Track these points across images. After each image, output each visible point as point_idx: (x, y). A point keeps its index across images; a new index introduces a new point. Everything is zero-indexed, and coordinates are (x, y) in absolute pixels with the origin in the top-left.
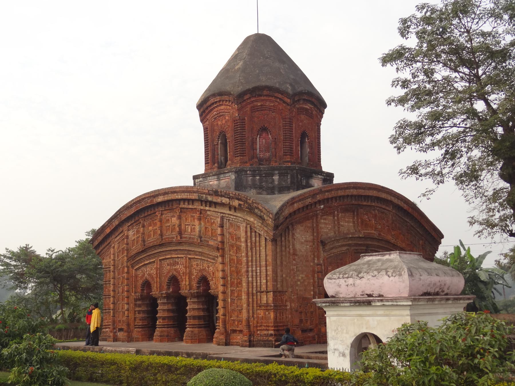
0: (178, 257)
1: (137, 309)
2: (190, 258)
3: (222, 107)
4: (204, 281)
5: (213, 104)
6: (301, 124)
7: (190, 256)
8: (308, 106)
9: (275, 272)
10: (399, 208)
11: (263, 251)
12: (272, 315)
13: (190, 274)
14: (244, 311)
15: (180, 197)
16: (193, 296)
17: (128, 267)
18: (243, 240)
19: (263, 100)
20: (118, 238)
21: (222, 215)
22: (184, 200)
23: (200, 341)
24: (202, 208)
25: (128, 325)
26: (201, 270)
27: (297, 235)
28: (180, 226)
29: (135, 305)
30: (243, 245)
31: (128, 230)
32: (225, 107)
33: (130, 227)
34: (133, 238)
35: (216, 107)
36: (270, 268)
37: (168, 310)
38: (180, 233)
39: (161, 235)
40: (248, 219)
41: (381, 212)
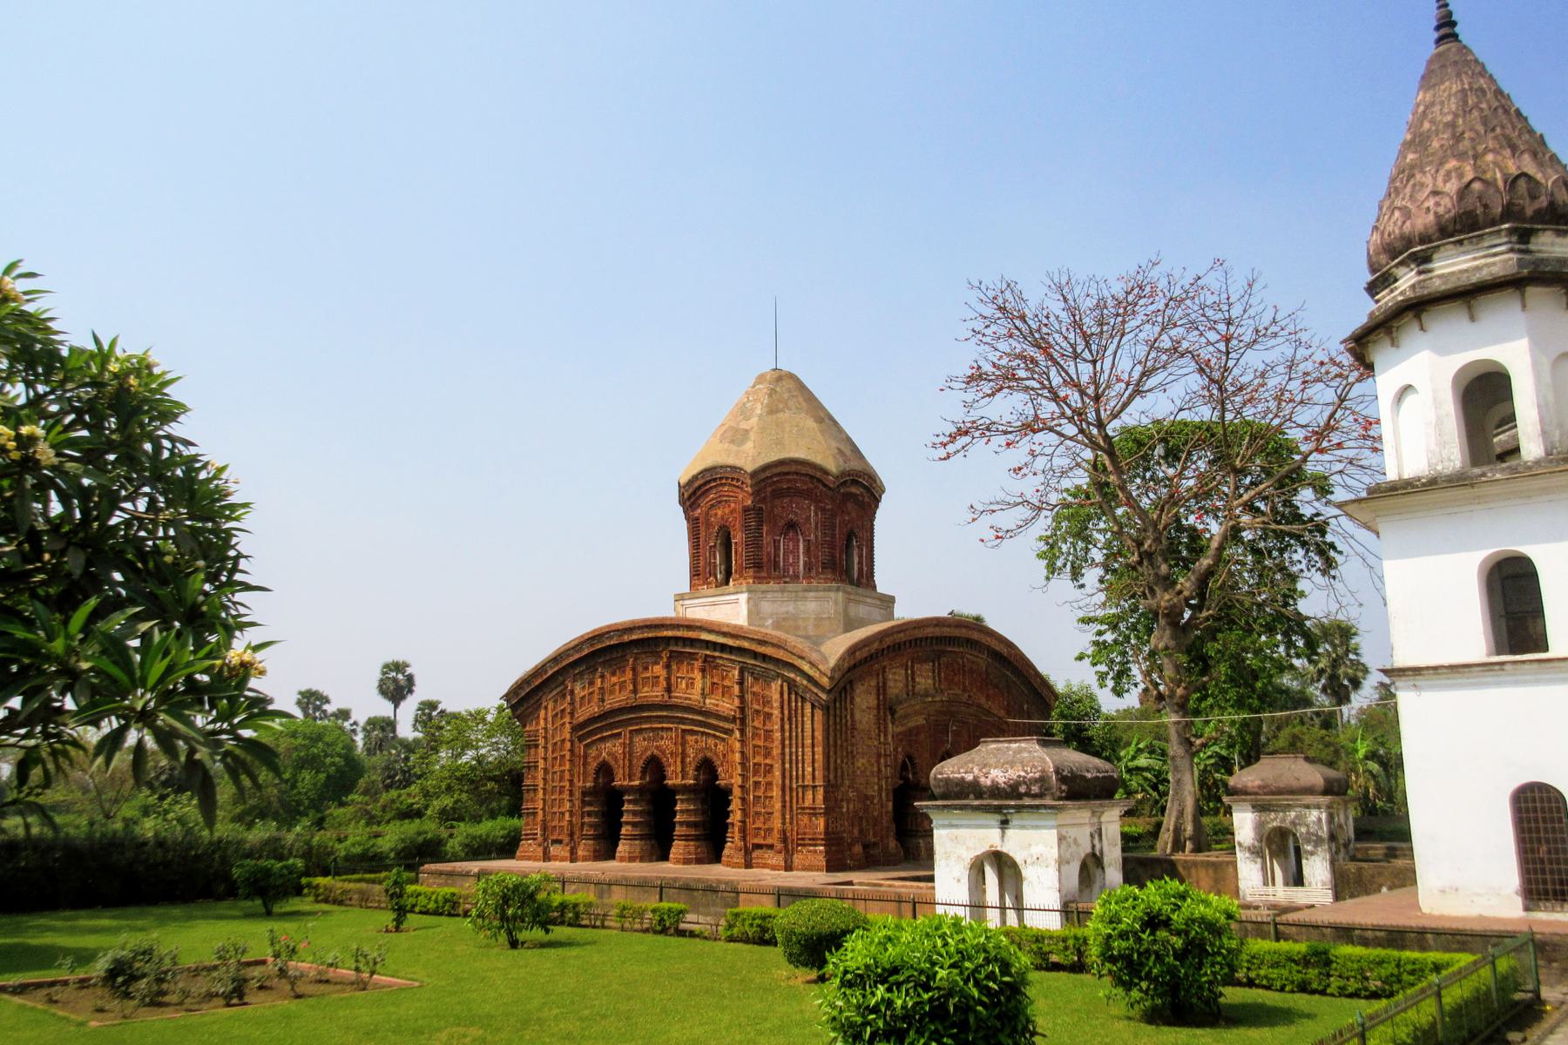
1: (587, 809)
4: (707, 767)
8: (854, 490)
9: (827, 756)
10: (996, 656)
11: (808, 725)
12: (821, 822)
13: (684, 755)
14: (777, 815)
16: (685, 789)
17: (572, 742)
18: (776, 705)
22: (677, 639)
23: (699, 861)
25: (571, 835)
26: (701, 750)
27: (858, 700)
28: (668, 679)
29: (583, 801)
30: (776, 712)
36: (819, 750)
37: (640, 813)
38: (669, 690)
39: (635, 691)
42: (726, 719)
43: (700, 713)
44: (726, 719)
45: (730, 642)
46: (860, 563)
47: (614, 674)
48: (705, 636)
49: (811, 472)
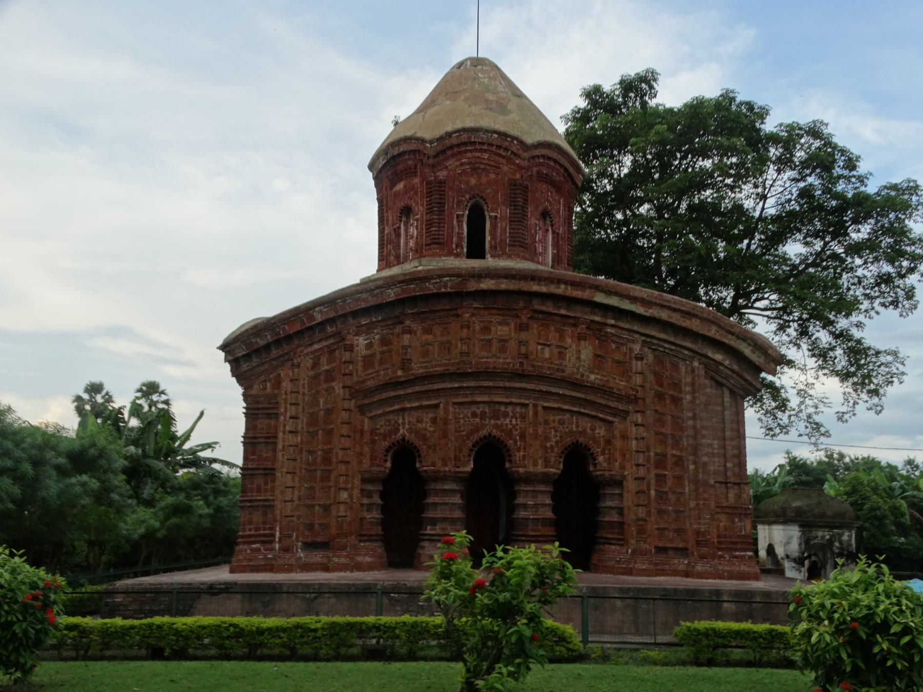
0: (511, 403)
2: (544, 408)
3: (486, 156)
5: (465, 144)
7: (546, 404)
15: (544, 289)
19: (548, 167)
20: (316, 347)
21: (643, 338)
24: (597, 319)
31: (357, 334)
32: (493, 157)
33: (364, 328)
34: (364, 352)
35: (471, 151)
40: (710, 354)
42: (620, 398)
43: (577, 385)
44: (620, 398)
45: (640, 310)
47: (428, 331)
48: (600, 298)
49: (567, 165)
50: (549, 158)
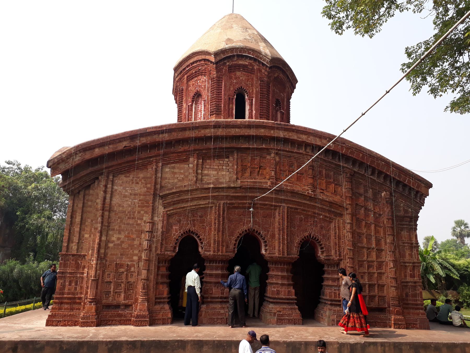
6: (235, 81)
19: (195, 67)
41: (286, 156)
46: (251, 110)
49: (203, 57)
50: (193, 63)
